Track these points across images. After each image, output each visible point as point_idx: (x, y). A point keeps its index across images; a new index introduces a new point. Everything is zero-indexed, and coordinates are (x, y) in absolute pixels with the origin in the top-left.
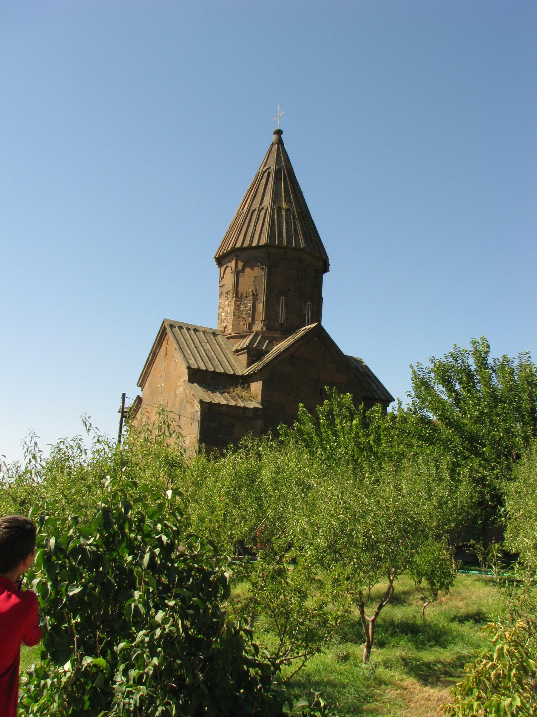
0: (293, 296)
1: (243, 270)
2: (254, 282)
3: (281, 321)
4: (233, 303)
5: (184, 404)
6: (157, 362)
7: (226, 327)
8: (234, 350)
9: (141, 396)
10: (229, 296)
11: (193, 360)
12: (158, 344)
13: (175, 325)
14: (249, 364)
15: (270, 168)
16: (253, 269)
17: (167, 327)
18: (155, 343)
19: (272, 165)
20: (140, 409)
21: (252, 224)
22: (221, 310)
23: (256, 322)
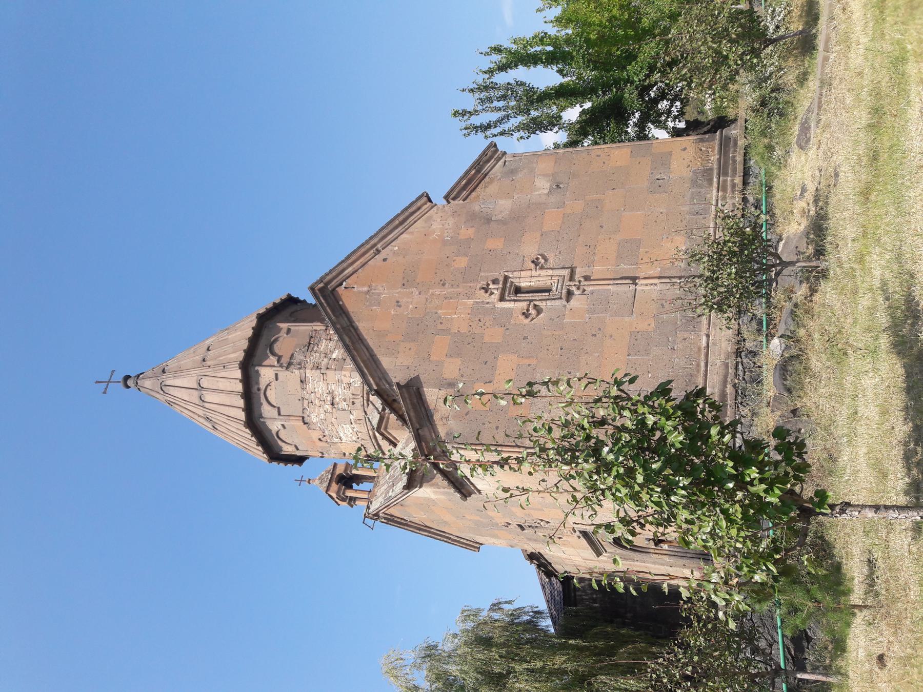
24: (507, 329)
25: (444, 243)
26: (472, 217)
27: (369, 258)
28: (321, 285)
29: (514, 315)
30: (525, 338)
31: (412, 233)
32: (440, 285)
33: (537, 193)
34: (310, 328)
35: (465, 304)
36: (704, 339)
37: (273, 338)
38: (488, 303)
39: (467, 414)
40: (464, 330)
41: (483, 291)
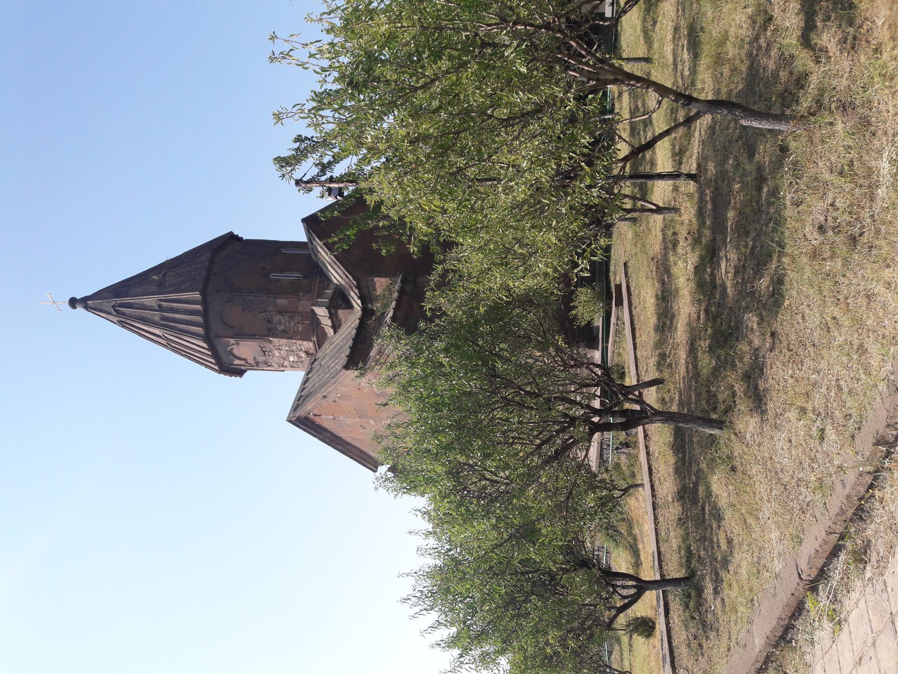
0: (271, 264)
2: (249, 312)
3: (301, 277)
4: (276, 341)
6: (343, 435)
7: (307, 353)
8: (332, 331)
10: (268, 349)
11: (337, 366)
13: (295, 405)
14: (349, 306)
15: (113, 307)
17: (297, 415)
19: (107, 305)
21: (177, 316)
22: (286, 363)
37: (229, 349)
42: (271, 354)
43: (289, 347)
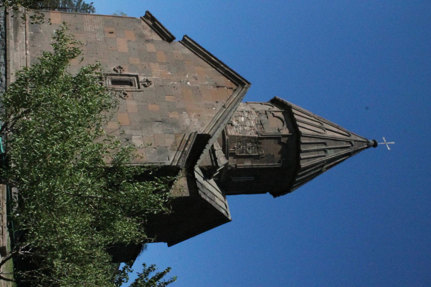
1: (280, 143)
2: (270, 154)
3: (233, 179)
5: (174, 130)
8: (215, 148)
9: (174, 41)
10: (259, 126)
12: (226, 72)
14: (201, 169)
15: (352, 145)
16: (279, 153)
17: (244, 89)
18: (227, 67)
20: (161, 39)
21: (316, 147)
22: (246, 114)
23: (235, 160)
24: (128, 63)
25: (185, 110)
26: (175, 124)
27: (227, 103)
28: (246, 86)
29: (127, 69)
30: (117, 59)
31: (209, 117)
32: (176, 87)
33: (139, 136)
34: (267, 132)
35: (157, 77)
36: (28, 52)
38: (144, 76)
39: (134, 30)
40: (152, 64)
41: (149, 80)
42: (257, 122)
43: (244, 130)
